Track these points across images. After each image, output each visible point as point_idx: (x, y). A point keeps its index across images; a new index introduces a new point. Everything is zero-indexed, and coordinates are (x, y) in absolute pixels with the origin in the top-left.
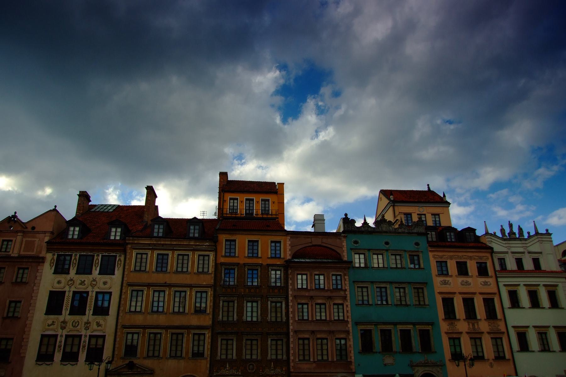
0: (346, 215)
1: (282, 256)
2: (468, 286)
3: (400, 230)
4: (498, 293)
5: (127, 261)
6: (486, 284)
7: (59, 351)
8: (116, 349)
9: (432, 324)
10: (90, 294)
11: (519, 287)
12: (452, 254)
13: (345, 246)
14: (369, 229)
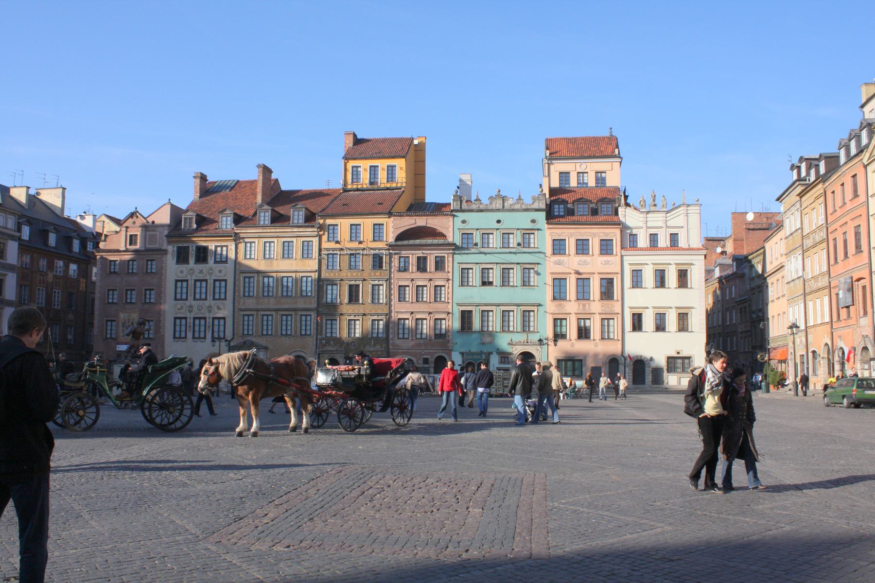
3: (517, 207)
6: (607, 263)
9: (540, 305)
12: (573, 231)
14: (482, 207)
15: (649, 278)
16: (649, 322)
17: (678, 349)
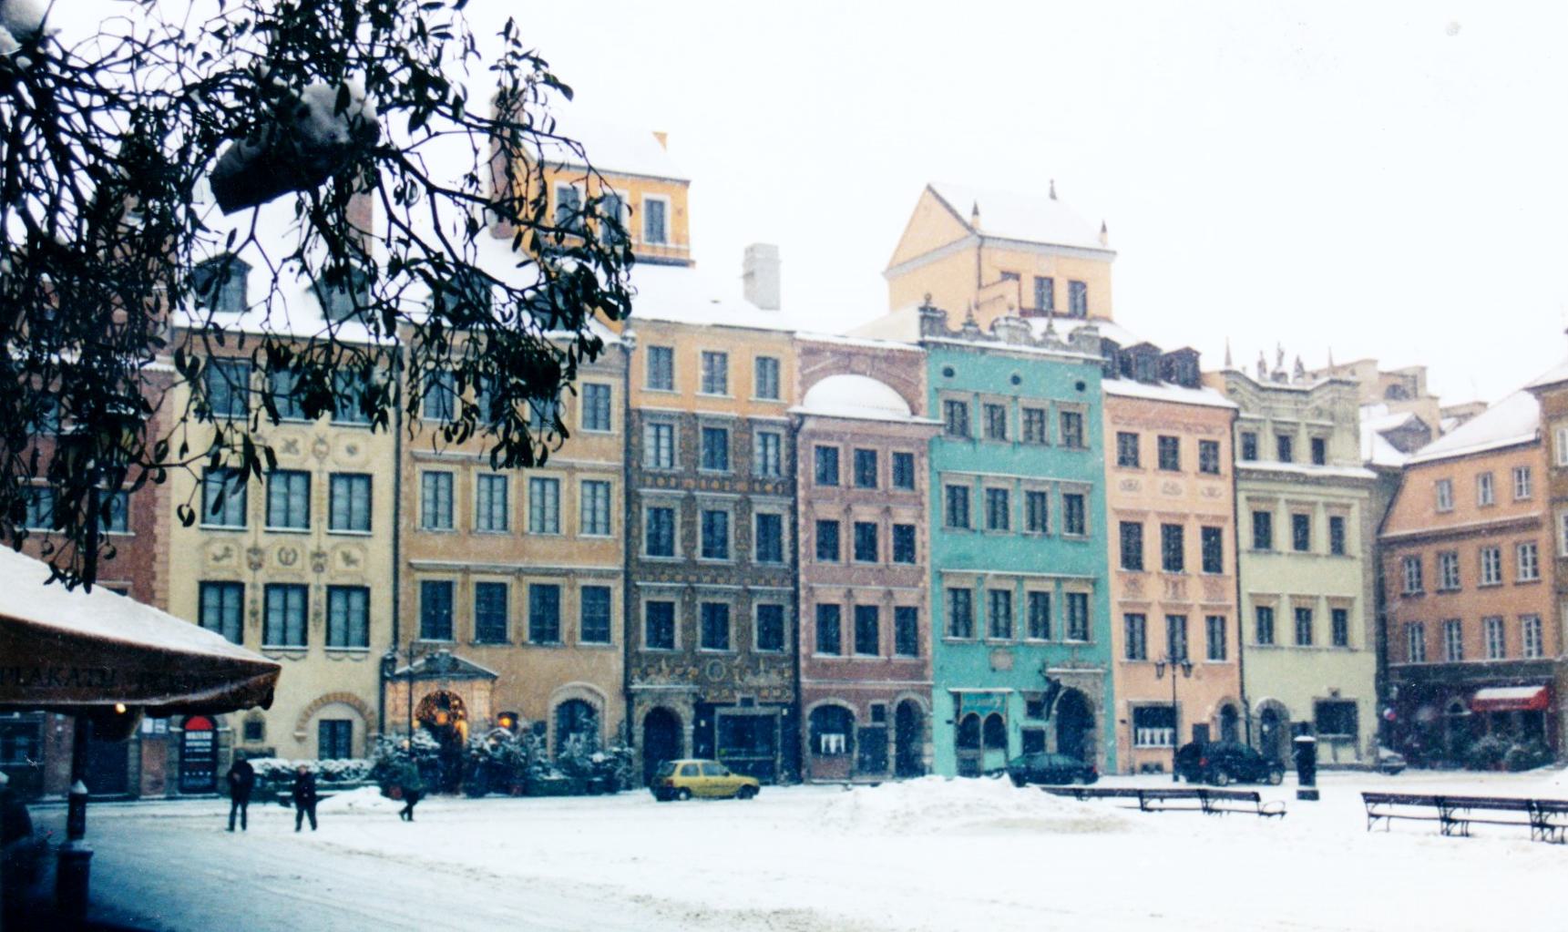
0: (928, 298)
6: (1211, 493)
8: (401, 622)
9: (1094, 583)
16: (1285, 626)
17: (1335, 685)
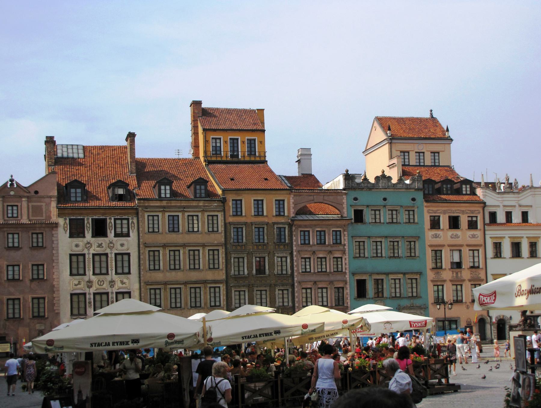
0: (347, 171)
1: (286, 214)
2: (457, 239)
3: (399, 186)
4: (483, 245)
5: (141, 224)
6: (473, 236)
7: (90, 307)
9: (420, 273)
10: (109, 255)
11: (504, 240)
12: (446, 209)
13: (345, 203)
14: (369, 185)
15: (507, 249)
